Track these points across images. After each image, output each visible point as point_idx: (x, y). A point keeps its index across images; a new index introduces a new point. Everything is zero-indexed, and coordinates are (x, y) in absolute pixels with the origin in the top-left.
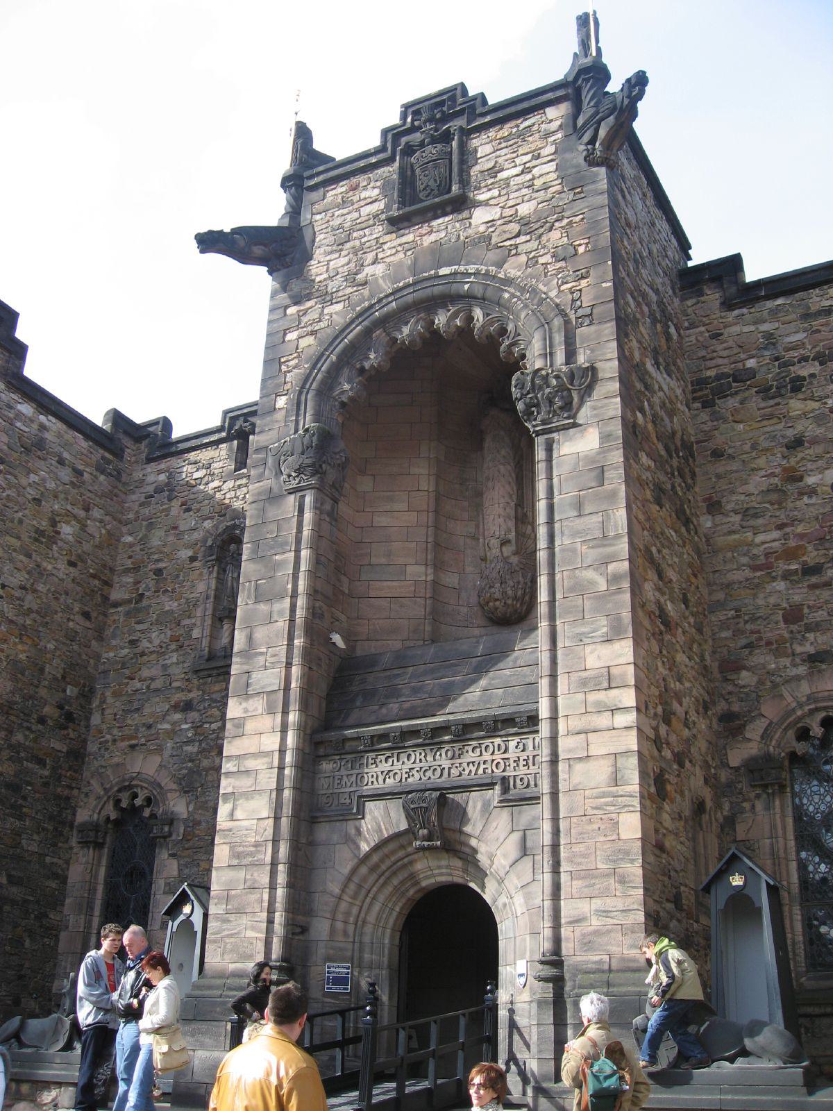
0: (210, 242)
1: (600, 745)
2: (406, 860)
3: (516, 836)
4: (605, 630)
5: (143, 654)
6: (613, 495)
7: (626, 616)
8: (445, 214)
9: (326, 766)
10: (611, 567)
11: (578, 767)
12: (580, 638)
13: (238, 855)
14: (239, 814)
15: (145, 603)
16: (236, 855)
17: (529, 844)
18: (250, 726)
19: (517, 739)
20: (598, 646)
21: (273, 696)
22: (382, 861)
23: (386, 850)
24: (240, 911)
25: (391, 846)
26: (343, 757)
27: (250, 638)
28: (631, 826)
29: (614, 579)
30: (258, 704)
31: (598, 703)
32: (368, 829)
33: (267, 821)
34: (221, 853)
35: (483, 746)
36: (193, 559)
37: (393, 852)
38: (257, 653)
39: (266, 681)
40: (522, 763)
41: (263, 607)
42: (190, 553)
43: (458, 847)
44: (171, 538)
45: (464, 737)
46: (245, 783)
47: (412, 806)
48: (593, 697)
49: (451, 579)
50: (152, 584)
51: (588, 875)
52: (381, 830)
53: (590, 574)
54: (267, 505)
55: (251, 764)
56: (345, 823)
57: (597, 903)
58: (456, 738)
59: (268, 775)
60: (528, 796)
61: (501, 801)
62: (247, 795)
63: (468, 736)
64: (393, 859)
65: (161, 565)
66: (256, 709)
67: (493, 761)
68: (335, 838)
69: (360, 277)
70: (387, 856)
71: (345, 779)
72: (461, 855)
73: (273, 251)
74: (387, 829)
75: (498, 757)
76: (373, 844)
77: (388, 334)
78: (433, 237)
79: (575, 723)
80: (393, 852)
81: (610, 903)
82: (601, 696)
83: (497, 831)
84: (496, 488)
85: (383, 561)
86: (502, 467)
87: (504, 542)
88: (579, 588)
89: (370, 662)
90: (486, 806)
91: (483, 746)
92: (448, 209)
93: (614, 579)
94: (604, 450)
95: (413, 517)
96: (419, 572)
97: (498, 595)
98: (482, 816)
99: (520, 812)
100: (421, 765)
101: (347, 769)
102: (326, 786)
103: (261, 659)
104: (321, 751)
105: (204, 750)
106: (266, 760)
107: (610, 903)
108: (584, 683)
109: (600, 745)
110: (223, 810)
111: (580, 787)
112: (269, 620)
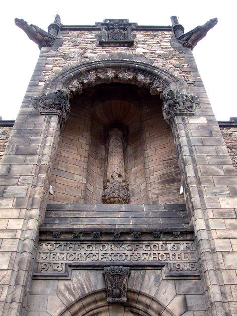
0: (20, 23)
2: (95, 311)
3: (179, 299)
4: (228, 192)
8: (124, 46)
9: (45, 247)
10: (224, 167)
11: (228, 257)
12: (215, 194)
17: (189, 304)
19: (173, 244)
20: (226, 198)
21: (21, 200)
22: (80, 310)
23: (85, 302)
25: (89, 300)
26: (58, 242)
27: (9, 170)
31: (231, 225)
32: (74, 288)
33: (6, 272)
35: (152, 246)
37: (89, 304)
38: (14, 178)
39: (17, 192)
40: (177, 256)
41: (20, 157)
43: (134, 304)
45: (139, 239)
47: (113, 273)
48: (228, 221)
49: (91, 187)
52: (84, 289)
53: (214, 168)
54: (29, 117)
56: (57, 281)
58: (135, 239)
59: (11, 243)
60: (185, 274)
61: (167, 276)
63: (143, 239)
64: (87, 309)
66: (8, 205)
67: (159, 254)
68: (49, 291)
69: (85, 55)
70: (84, 307)
71: (58, 255)
72: (135, 310)
73: (45, 39)
74: (88, 288)
75: (162, 252)
76: (77, 297)
77: (97, 74)
78: (119, 51)
79: (220, 233)
80: (89, 304)
83: (166, 294)
84: (116, 156)
85: (64, 169)
86: (119, 149)
87: (120, 176)
89: (59, 209)
90: (157, 279)
91: (152, 246)
92: (126, 45)
95: (79, 157)
96: (80, 179)
97: (116, 195)
98: (155, 284)
99: (180, 284)
100: (112, 252)
101: (60, 250)
102: (44, 258)
103: (15, 181)
104: (43, 238)
106: (11, 234)
108: (222, 215)
111: (232, 267)
112: (24, 163)
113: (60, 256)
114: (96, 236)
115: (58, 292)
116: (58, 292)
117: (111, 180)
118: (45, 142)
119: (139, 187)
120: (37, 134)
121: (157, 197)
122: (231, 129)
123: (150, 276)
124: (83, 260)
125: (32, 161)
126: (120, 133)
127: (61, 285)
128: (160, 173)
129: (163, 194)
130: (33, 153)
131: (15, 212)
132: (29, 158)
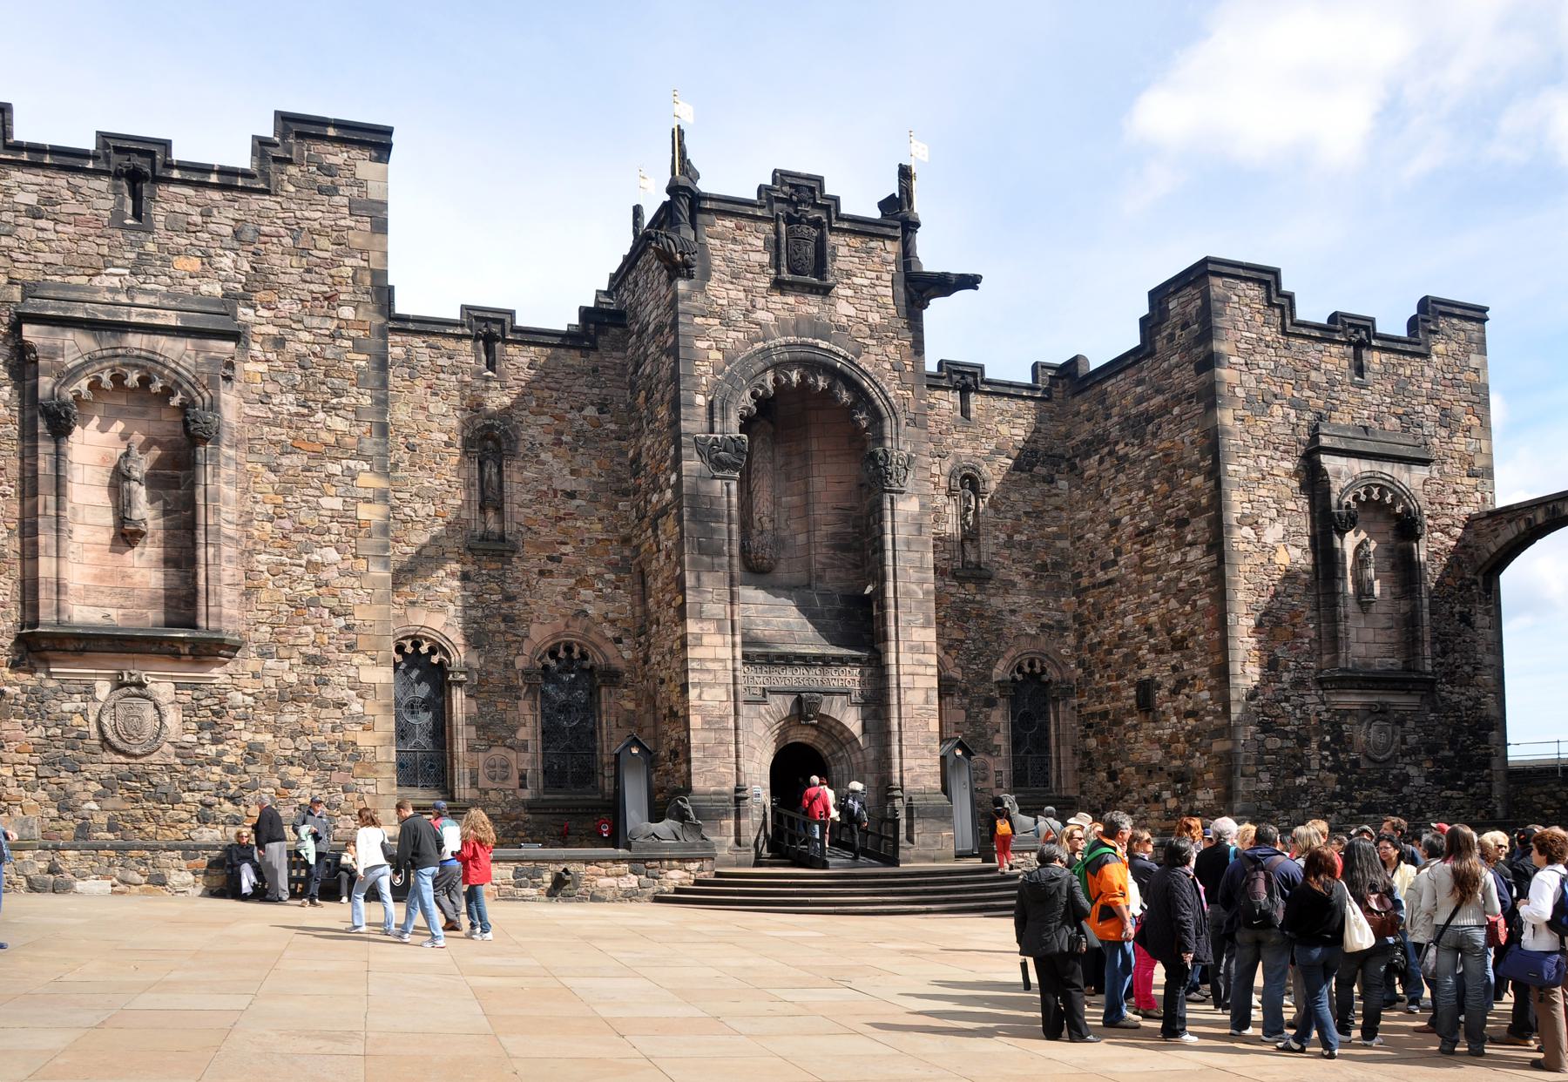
1: (921, 682)
5: (403, 522)
6: (925, 543)
7: (933, 616)
13: (708, 722)
14: (705, 696)
15: (399, 474)
16: (704, 721)
18: (706, 640)
24: (714, 756)
28: (934, 725)
29: (926, 593)
30: (710, 627)
34: (695, 721)
36: (448, 445)
41: (706, 559)
42: (446, 438)
44: (421, 417)
46: (708, 677)
48: (916, 656)
50: (406, 457)
51: (914, 748)
53: (914, 587)
55: (710, 665)
57: (919, 762)
62: (711, 686)
65: (411, 440)
81: (925, 762)
82: (921, 656)
88: (908, 593)
90: (842, 706)
93: (926, 593)
94: (921, 514)
103: (709, 596)
105: (487, 616)
107: (925, 762)
108: (911, 648)
109: (921, 682)
110: (693, 694)
113: (761, 678)
114: (788, 660)
115: (760, 715)
116: (760, 715)
117: (756, 524)
118: (730, 532)
119: (793, 536)
120: (717, 517)
121: (824, 570)
122: (938, 393)
123: (838, 701)
124: (781, 685)
125: (721, 566)
126: (771, 429)
127: (762, 708)
128: (830, 529)
129: (832, 566)
130: (720, 553)
131: (718, 639)
132: (716, 561)
